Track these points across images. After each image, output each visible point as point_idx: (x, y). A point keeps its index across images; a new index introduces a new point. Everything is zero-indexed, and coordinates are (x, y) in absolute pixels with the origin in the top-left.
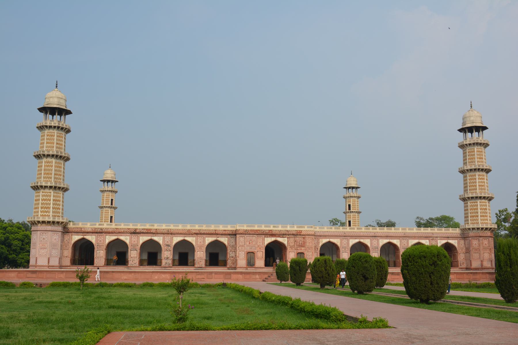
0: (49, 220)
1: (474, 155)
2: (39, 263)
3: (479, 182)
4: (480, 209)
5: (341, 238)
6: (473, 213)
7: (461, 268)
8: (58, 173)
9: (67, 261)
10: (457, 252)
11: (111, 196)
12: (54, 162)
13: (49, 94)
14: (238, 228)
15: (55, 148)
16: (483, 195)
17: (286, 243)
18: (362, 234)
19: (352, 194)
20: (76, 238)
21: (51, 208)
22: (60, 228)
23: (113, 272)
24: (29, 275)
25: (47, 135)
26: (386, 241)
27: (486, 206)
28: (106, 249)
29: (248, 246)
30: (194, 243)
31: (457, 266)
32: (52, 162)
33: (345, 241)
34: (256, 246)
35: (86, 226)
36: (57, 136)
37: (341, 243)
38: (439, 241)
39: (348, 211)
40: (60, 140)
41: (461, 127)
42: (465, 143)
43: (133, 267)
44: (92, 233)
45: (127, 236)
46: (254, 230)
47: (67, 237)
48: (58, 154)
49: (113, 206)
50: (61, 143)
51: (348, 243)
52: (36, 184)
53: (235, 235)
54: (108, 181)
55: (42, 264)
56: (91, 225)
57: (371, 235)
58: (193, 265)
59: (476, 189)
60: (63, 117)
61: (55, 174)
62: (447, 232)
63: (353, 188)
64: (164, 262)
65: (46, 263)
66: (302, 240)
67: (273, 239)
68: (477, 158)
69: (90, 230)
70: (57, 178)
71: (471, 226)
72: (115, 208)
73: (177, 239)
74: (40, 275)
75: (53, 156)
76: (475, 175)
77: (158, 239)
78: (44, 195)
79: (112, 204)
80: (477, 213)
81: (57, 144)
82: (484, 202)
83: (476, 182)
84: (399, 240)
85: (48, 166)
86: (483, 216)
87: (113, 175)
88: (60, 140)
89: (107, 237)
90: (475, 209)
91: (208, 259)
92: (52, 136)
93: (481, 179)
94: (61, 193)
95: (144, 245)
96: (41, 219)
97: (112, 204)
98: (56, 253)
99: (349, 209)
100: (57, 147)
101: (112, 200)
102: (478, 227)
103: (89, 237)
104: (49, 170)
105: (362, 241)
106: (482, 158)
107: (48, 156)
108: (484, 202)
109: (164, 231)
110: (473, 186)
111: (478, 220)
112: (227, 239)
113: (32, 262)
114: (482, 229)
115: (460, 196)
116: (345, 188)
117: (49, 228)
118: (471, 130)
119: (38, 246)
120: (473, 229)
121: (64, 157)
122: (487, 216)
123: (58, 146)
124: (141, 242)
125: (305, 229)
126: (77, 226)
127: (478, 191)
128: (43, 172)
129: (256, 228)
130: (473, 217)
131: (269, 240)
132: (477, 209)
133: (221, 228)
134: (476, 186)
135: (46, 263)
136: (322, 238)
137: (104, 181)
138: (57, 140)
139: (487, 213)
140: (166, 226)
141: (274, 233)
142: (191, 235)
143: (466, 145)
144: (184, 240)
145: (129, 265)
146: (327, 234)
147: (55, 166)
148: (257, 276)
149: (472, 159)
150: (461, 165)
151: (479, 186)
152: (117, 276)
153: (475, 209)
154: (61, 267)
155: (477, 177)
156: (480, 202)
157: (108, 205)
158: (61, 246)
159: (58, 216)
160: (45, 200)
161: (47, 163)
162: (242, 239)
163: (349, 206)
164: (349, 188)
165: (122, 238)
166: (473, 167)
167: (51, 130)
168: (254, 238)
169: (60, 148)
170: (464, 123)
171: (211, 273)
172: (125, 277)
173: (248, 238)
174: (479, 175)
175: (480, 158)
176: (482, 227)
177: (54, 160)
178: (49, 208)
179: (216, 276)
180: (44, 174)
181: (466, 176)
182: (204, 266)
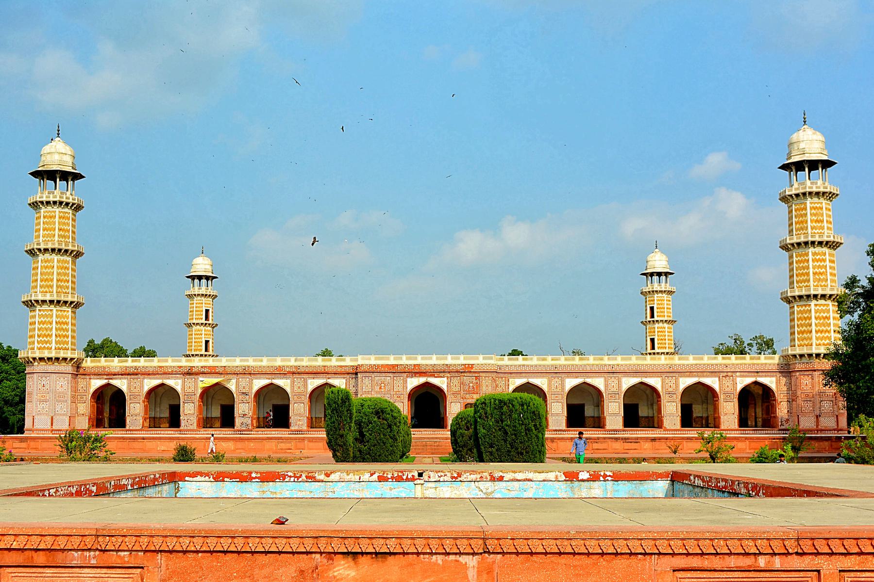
0: (50, 356)
1: (806, 215)
2: (36, 426)
3: (814, 268)
4: (816, 318)
5: (550, 375)
6: (802, 325)
7: (783, 430)
9: (83, 423)
10: (775, 400)
14: (360, 362)
15: (56, 238)
17: (444, 387)
20: (97, 383)
22: (69, 368)
25: (44, 217)
26: (633, 381)
27: (828, 311)
28: (144, 402)
30: (288, 390)
31: (773, 427)
33: (556, 382)
34: (392, 393)
35: (112, 364)
36: (60, 218)
38: (738, 379)
40: (64, 224)
43: (189, 430)
45: (177, 378)
47: (81, 382)
48: (60, 247)
51: (563, 385)
53: (356, 374)
55: (42, 427)
57: (606, 370)
59: (809, 281)
62: (755, 362)
64: (238, 421)
67: (422, 380)
68: (812, 221)
70: (61, 287)
71: (798, 351)
73: (259, 383)
75: (53, 250)
76: (807, 255)
81: (60, 230)
82: (824, 305)
84: (659, 379)
85: (46, 267)
86: (822, 332)
88: (64, 224)
90: (805, 319)
96: (37, 355)
98: (63, 409)
102: (810, 352)
103: (117, 383)
104: (49, 274)
105: (589, 381)
108: (824, 305)
110: (803, 274)
111: (811, 339)
112: (344, 381)
113: (28, 424)
117: (51, 368)
118: (799, 166)
120: (802, 356)
121: (72, 251)
122: (829, 332)
125: (479, 360)
126: (98, 364)
129: (392, 360)
130: (803, 332)
131: (414, 382)
132: (810, 318)
134: (808, 274)
136: (514, 378)
140: (241, 361)
141: (423, 369)
142: (282, 376)
146: (523, 369)
149: (802, 222)
151: (815, 274)
153: (805, 319)
155: (810, 257)
156: (816, 305)
158: (73, 397)
161: (46, 262)
162: (367, 381)
165: (171, 382)
166: (802, 239)
167: (49, 208)
169: (65, 237)
173: (378, 378)
174: (814, 254)
175: (817, 221)
176: (817, 352)
177: (55, 257)
178: (51, 336)
179: (311, 444)
180: (42, 281)
181: (791, 257)
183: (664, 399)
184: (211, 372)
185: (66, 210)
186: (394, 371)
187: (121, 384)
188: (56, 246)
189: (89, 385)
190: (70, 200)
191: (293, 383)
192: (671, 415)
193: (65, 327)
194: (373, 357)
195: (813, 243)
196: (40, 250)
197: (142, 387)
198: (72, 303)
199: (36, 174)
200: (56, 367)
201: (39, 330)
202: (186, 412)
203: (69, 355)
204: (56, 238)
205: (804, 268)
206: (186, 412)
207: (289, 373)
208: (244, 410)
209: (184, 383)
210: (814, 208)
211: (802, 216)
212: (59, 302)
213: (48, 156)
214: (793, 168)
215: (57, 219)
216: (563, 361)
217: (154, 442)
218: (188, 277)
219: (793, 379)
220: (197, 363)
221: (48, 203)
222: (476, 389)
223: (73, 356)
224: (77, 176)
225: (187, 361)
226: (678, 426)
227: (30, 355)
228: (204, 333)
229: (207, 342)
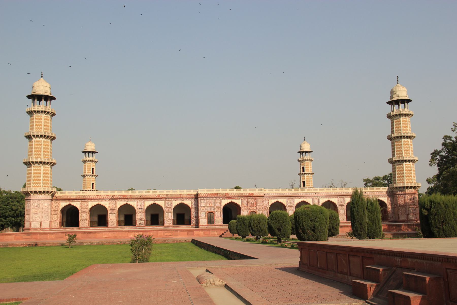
1: (400, 124)
3: (404, 148)
6: (399, 174)
8: (46, 150)
9: (56, 224)
11: (92, 165)
12: (42, 141)
13: (36, 84)
15: (43, 130)
16: (408, 159)
18: (305, 195)
19: (305, 158)
20: (63, 204)
21: (42, 180)
22: (49, 196)
23: (95, 232)
24: (25, 237)
27: (411, 167)
29: (208, 207)
30: (163, 206)
32: (41, 141)
33: (290, 201)
34: (215, 207)
36: (45, 119)
37: (287, 202)
39: (302, 172)
41: (389, 100)
42: (392, 114)
44: (77, 200)
46: (213, 194)
47: (55, 204)
48: (45, 134)
49: (94, 174)
50: (47, 124)
52: (28, 161)
53: (198, 198)
54: (89, 152)
56: (76, 193)
57: (313, 195)
58: (163, 224)
59: (402, 154)
60: (49, 102)
61: (44, 152)
63: (306, 152)
64: (138, 222)
65: (39, 227)
66: (254, 201)
67: (229, 201)
69: (75, 197)
70: (45, 155)
72: (96, 176)
73: (148, 203)
74: (34, 236)
75: (41, 136)
76: (401, 142)
77: (133, 203)
78: (35, 170)
79: (93, 172)
80: (403, 174)
81: (45, 125)
82: (409, 165)
83: (401, 148)
84: (337, 199)
85: (37, 145)
86: (408, 176)
87: (93, 147)
89: (90, 203)
90: (401, 171)
91: (175, 219)
92: (40, 119)
93: (406, 145)
94: (49, 167)
95: (121, 209)
96: (33, 190)
97: (93, 172)
98: (46, 217)
99: (304, 171)
100: (44, 129)
101: (93, 169)
102: (404, 186)
103: (74, 204)
104: (39, 148)
105: (305, 200)
106: (407, 127)
107: (38, 136)
108: (409, 165)
109: (137, 197)
110: (399, 151)
111: (404, 180)
112: (190, 201)
113: (27, 225)
114: (407, 187)
115: (389, 160)
116: (299, 152)
117: (40, 196)
118: (397, 102)
119: (32, 212)
120: (400, 187)
121: (51, 137)
122: (411, 176)
123: (45, 127)
124: (118, 206)
125: (256, 192)
127: (403, 155)
128: (33, 150)
129: (215, 192)
130: (400, 177)
132: (403, 170)
133: (185, 193)
134: (402, 151)
135: (39, 227)
137: (85, 152)
138: (44, 122)
139: (411, 173)
141: (229, 195)
143: (393, 115)
144: (154, 204)
145: (109, 226)
146: (275, 195)
147: (44, 145)
148: (216, 232)
149: (398, 127)
150: (390, 133)
152: (99, 235)
153: (401, 171)
154: (51, 229)
155: (403, 143)
156: (405, 165)
157: (90, 174)
158: (51, 211)
159: (48, 187)
160: (36, 173)
161: (37, 142)
163: (303, 168)
164: (303, 152)
165: (103, 203)
166: (399, 135)
167: (38, 114)
168: (213, 200)
169: (46, 129)
170: (391, 97)
171: (177, 230)
172: (106, 236)
173: (208, 200)
175: (405, 127)
178: (40, 180)
179: (181, 233)
180: (35, 152)
182: (171, 225)
183: (339, 208)
184: (124, 198)
185: (47, 115)
186: (216, 196)
187: (77, 204)
188: (43, 134)
189: (59, 205)
190: (50, 111)
191: (165, 203)
192: (342, 215)
193: (47, 175)
194: (206, 190)
195: (404, 136)
196: (34, 136)
197: (87, 206)
198: (51, 163)
199: (30, 97)
200: (43, 196)
201: (34, 177)
202: (111, 218)
203: (50, 190)
204: (43, 130)
205: (399, 148)
206: (111, 218)
207: (163, 198)
208: (140, 217)
209: (110, 203)
210: (404, 121)
211: (398, 124)
212: (44, 162)
213: (38, 88)
214: (394, 103)
215: (43, 120)
216: (293, 191)
217: (101, 233)
218: (82, 152)
219: (395, 198)
220: (87, 194)
221: (38, 112)
222: (255, 205)
223: (52, 190)
224: (53, 98)
225: (83, 193)
226: (345, 221)
227: (29, 190)
228: (91, 180)
229: (93, 184)
